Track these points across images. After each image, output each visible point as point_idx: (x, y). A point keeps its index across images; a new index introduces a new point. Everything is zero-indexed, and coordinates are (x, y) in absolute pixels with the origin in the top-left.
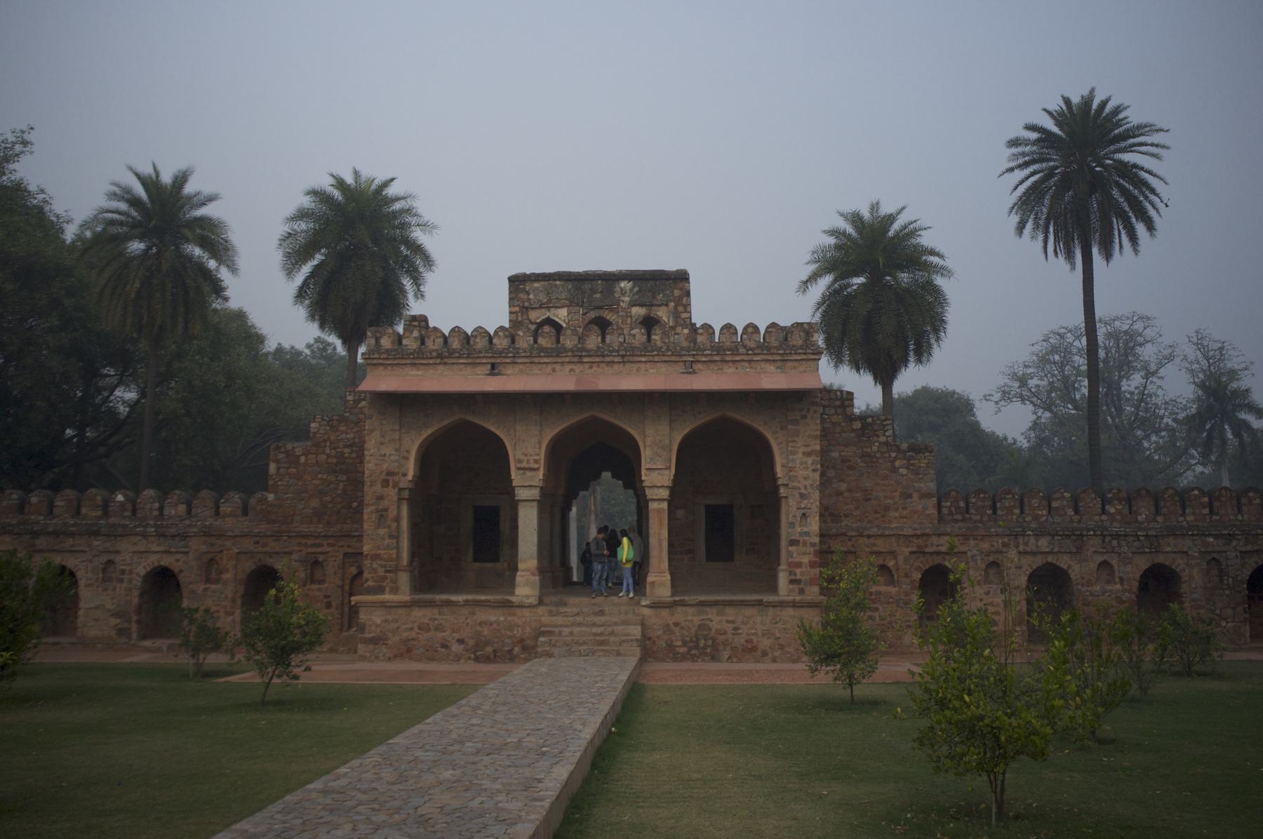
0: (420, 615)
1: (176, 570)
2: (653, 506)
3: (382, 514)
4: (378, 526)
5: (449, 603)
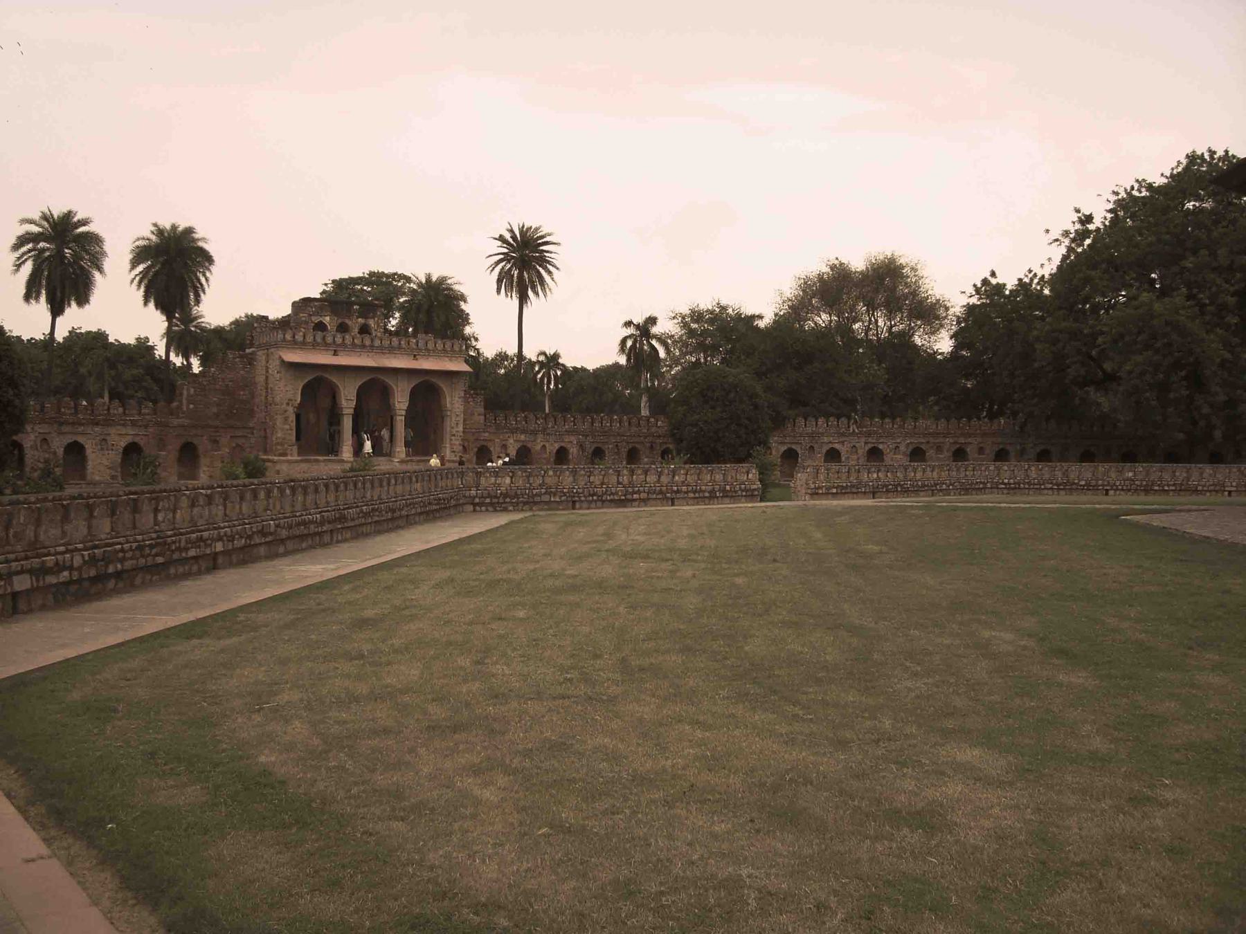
0: (304, 466)
1: (142, 445)
2: (399, 418)
3: (286, 419)
4: (285, 424)
5: (317, 461)
